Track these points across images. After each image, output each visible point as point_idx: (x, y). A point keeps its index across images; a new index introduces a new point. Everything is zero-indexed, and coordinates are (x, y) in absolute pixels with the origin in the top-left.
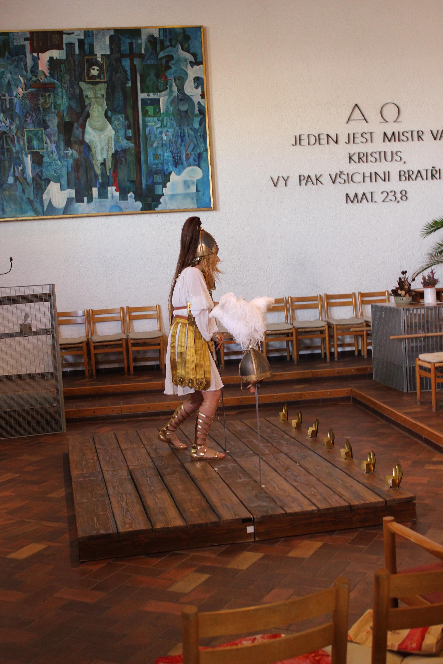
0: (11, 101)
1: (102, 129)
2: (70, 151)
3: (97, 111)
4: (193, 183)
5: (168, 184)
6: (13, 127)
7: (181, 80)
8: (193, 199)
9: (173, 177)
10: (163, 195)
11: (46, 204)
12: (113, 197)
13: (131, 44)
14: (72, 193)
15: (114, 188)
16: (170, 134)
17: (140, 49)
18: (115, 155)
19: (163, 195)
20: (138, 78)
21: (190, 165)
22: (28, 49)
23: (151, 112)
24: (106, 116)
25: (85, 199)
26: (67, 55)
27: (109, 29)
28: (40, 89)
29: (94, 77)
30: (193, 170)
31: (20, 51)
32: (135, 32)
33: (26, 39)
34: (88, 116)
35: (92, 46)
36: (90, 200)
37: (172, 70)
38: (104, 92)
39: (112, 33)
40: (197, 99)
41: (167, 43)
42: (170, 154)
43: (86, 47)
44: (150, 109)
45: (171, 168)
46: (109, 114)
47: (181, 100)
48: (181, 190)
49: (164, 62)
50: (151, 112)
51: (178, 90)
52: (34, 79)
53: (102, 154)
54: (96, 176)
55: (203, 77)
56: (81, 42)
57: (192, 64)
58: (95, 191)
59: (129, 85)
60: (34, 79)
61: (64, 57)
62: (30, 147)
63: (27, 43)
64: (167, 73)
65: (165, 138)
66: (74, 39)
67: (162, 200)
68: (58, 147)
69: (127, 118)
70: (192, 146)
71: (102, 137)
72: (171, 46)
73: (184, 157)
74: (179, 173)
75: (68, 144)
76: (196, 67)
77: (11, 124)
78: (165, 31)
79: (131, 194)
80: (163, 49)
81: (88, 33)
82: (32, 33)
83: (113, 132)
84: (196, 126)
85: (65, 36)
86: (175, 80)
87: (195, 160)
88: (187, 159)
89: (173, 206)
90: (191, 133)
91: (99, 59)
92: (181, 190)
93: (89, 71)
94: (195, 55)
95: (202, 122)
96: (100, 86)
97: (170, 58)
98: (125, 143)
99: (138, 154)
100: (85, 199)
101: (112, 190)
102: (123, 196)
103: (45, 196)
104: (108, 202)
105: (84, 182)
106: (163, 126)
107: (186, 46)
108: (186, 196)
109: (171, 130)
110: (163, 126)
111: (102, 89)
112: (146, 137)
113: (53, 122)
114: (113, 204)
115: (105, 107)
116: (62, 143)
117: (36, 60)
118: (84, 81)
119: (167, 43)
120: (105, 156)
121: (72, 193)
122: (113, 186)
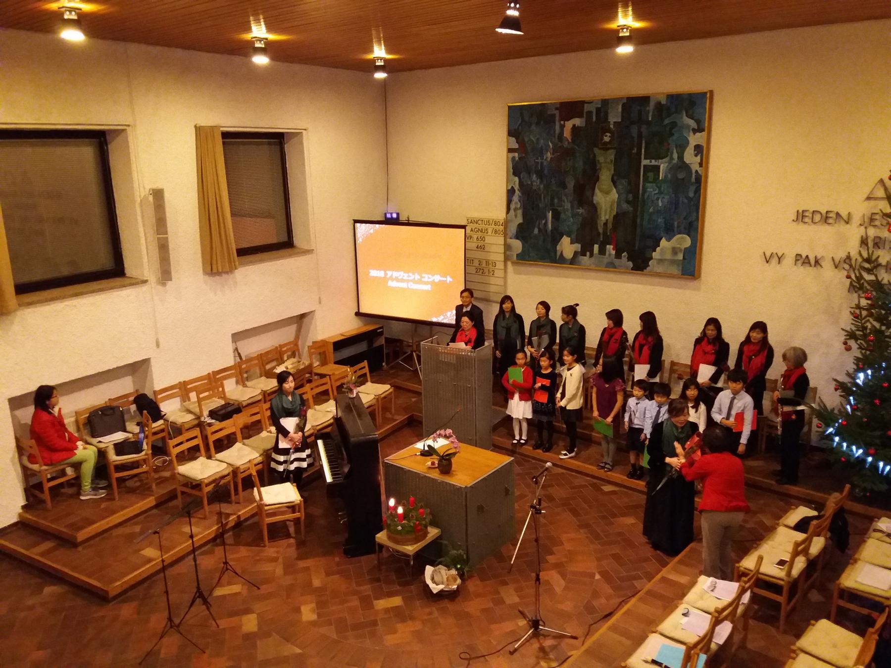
0: (542, 163)
1: (608, 193)
2: (581, 211)
3: (605, 176)
4: (681, 251)
5: (658, 249)
6: (542, 186)
7: (682, 147)
8: (678, 265)
9: (664, 243)
10: (652, 258)
11: (558, 254)
12: (610, 255)
13: (640, 112)
14: (577, 247)
15: (612, 247)
16: (666, 201)
17: (648, 117)
18: (615, 217)
19: (652, 258)
20: (643, 145)
21: (680, 233)
22: (557, 118)
23: (651, 179)
24: (613, 180)
25: (588, 253)
26: (586, 121)
27: (622, 98)
28: (564, 153)
29: (606, 143)
30: (682, 238)
31: (550, 120)
32: (645, 100)
33: (557, 109)
34: (598, 179)
35: (606, 114)
36: (592, 255)
37: (675, 138)
38: (612, 157)
39: (625, 101)
40: (695, 167)
41: (673, 110)
42: (663, 221)
43: (602, 114)
44: (651, 175)
45: (662, 234)
46: (615, 178)
47: (680, 167)
48: (668, 256)
49: (668, 129)
50: (651, 179)
51: (678, 157)
52: (560, 144)
53: (605, 215)
54: (599, 234)
55: (705, 145)
56: (598, 109)
57: (695, 131)
58: (596, 247)
59: (635, 151)
60: (560, 144)
61: (584, 125)
62: (552, 204)
63: (557, 113)
64: (670, 140)
65: (660, 205)
66: (592, 108)
67: (650, 263)
68: (572, 207)
69: (629, 183)
70: (685, 214)
71: (607, 199)
72: (676, 112)
73: (676, 224)
74: (669, 240)
75: (581, 204)
76: (698, 134)
77: (541, 183)
78: (672, 97)
79: (625, 254)
80: (668, 116)
81: (605, 102)
82: (561, 103)
83: (617, 196)
84: (691, 195)
85: (586, 105)
86: (676, 147)
87: (685, 228)
88: (678, 227)
89: (660, 269)
90: (686, 201)
91: (612, 126)
92: (668, 256)
93: (602, 139)
94: (698, 122)
95: (698, 191)
96: (610, 151)
97: (674, 124)
98: (625, 206)
99: (635, 217)
100: (588, 253)
101: (610, 248)
102: (618, 255)
103: (558, 248)
104: (605, 259)
105: (590, 238)
106: (660, 193)
107: (691, 112)
108: (673, 262)
109: (667, 197)
110: (660, 193)
111: (611, 155)
112: (644, 201)
113: (571, 184)
114: (609, 260)
115: (613, 172)
116: (576, 202)
117: (562, 127)
118: (597, 147)
119: (673, 110)
120: (607, 217)
121: (577, 247)
122: (610, 244)
